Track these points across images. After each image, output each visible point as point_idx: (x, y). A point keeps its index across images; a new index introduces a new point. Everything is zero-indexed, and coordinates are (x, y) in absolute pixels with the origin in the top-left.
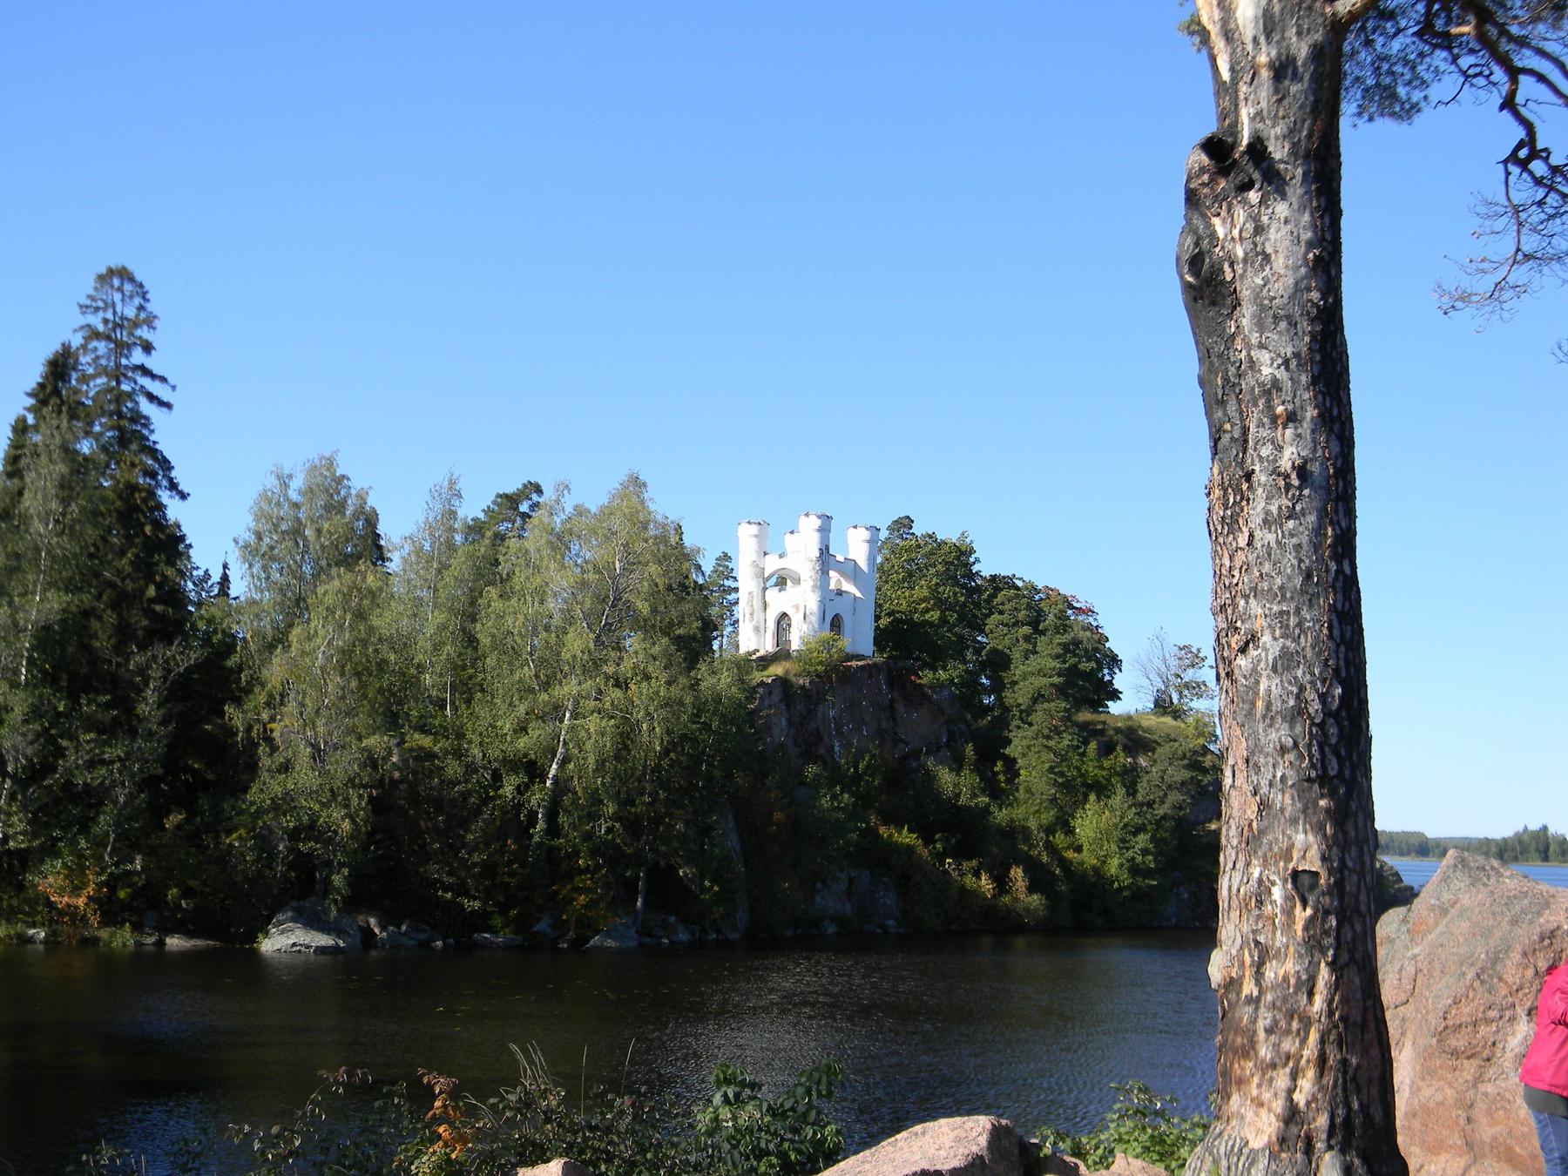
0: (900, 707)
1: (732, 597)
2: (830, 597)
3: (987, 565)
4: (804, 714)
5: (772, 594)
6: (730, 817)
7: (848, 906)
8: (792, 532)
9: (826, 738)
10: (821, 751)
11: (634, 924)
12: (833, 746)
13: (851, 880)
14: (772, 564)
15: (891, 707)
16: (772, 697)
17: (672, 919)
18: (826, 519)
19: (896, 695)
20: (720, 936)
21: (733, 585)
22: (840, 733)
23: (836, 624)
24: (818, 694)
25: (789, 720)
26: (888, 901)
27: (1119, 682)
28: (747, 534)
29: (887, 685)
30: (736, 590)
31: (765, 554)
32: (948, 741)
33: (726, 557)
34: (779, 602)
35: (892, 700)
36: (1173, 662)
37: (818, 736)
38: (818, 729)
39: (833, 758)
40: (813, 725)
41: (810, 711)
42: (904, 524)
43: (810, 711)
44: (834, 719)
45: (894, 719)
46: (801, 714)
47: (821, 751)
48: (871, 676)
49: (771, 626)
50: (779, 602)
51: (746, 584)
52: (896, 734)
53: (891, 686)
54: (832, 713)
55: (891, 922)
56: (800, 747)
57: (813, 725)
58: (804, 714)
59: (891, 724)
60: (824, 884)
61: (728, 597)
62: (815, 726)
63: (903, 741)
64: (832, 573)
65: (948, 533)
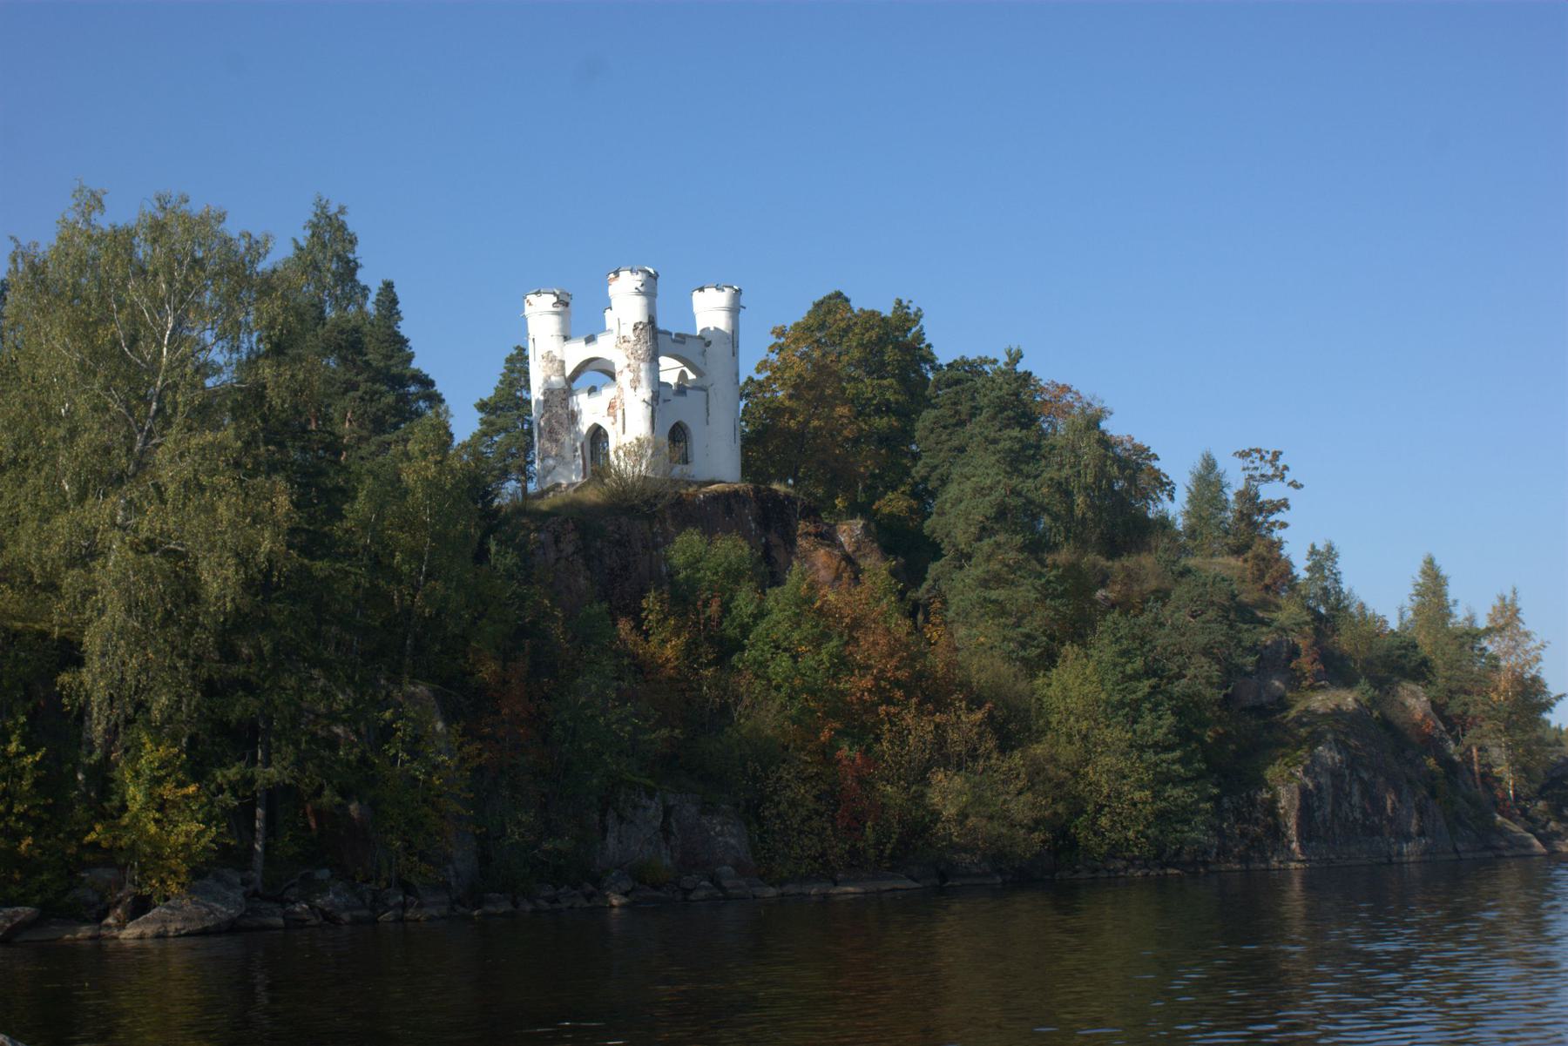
2: (660, 396)
13: (668, 811)
18: (652, 278)
19: (774, 538)
26: (733, 841)
28: (541, 316)
31: (566, 338)
60: (621, 819)
64: (665, 362)
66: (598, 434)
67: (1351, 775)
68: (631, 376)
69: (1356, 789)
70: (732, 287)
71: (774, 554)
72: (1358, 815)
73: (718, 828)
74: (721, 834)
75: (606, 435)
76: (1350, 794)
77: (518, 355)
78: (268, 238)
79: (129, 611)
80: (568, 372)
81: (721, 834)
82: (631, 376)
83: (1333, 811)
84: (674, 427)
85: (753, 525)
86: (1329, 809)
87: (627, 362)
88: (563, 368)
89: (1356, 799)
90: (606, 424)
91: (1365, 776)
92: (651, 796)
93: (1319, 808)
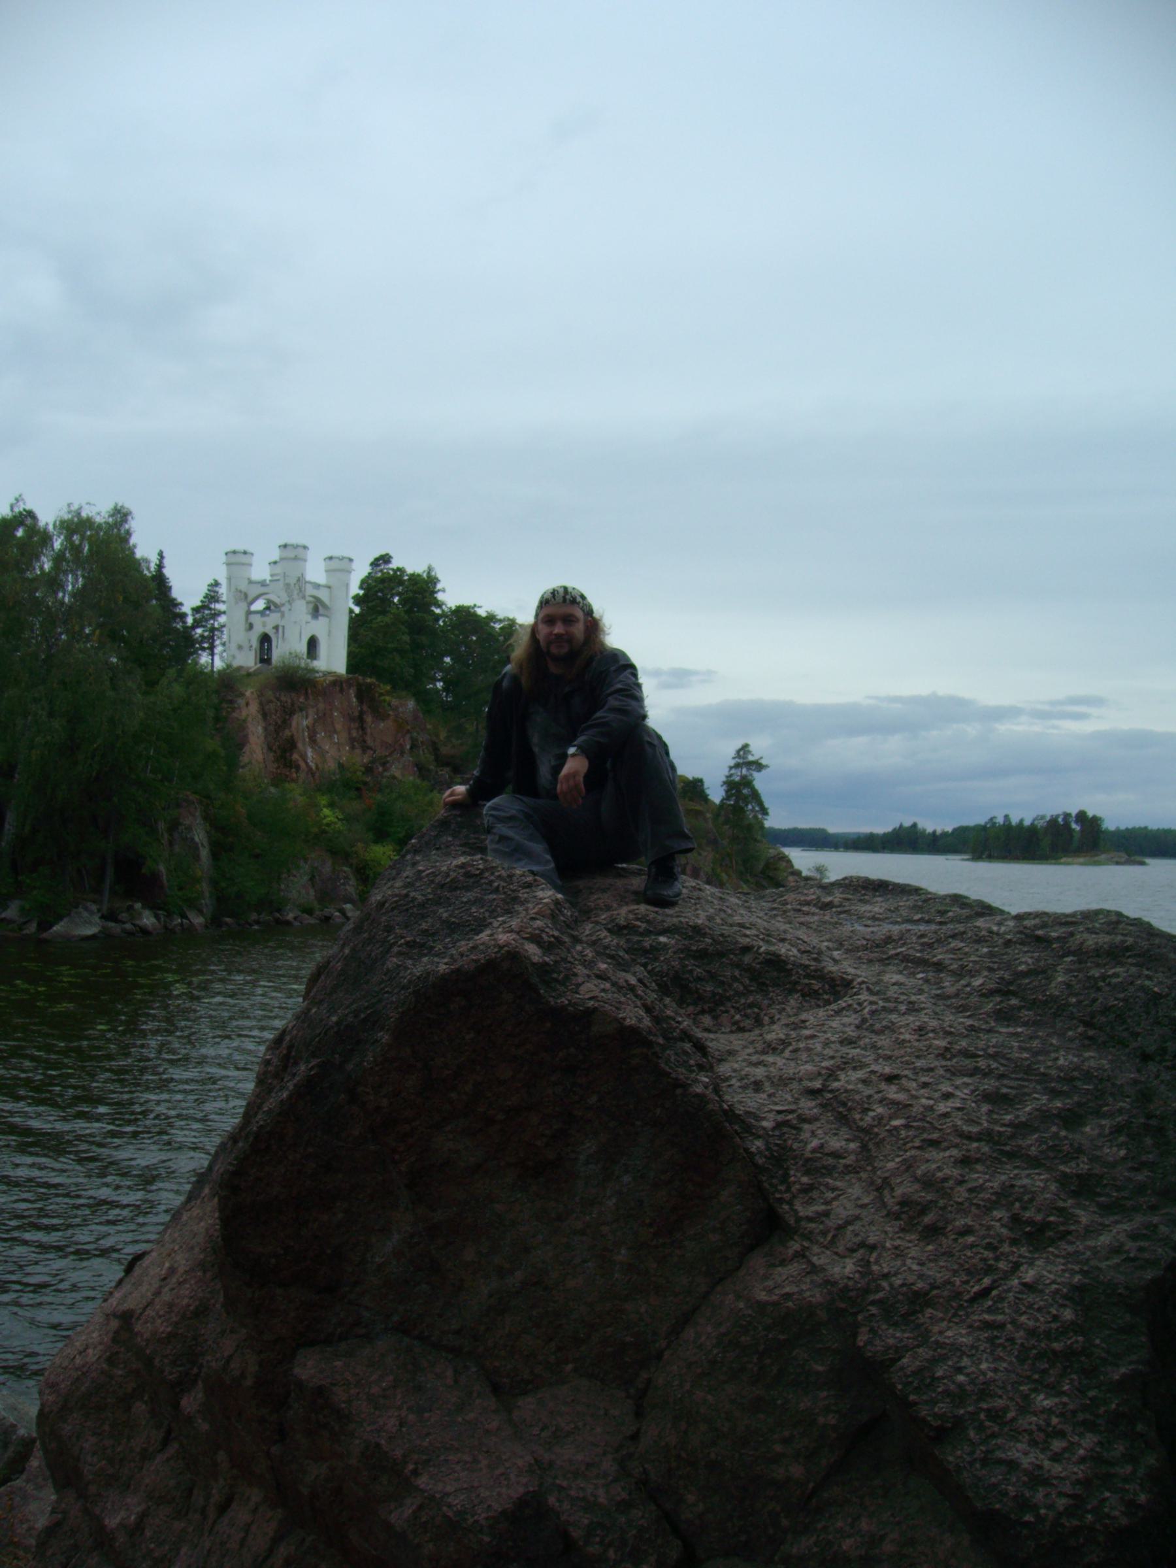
0: (369, 719)
1: (222, 619)
4: (279, 723)
6: (198, 814)
7: (312, 892)
8: (275, 563)
9: (300, 745)
10: (295, 756)
11: (99, 910)
12: (306, 753)
15: (361, 719)
17: (138, 906)
19: (365, 708)
20: (185, 921)
22: (313, 740)
23: (313, 643)
24: (293, 705)
25: (265, 729)
32: (411, 748)
33: (217, 584)
35: (362, 713)
37: (291, 745)
38: (292, 736)
39: (307, 763)
40: (287, 733)
41: (284, 722)
42: (385, 559)
43: (284, 722)
44: (308, 727)
45: (363, 729)
46: (276, 723)
47: (295, 756)
49: (255, 643)
52: (364, 741)
53: (360, 697)
54: (305, 723)
55: (348, 906)
56: (275, 752)
57: (287, 733)
58: (279, 723)
59: (360, 732)
62: (289, 734)
63: (369, 748)
66: (265, 639)
71: (365, 717)
73: (342, 881)
74: (344, 884)
80: (250, 598)
81: (344, 884)
85: (354, 700)
90: (271, 633)
92: (306, 863)
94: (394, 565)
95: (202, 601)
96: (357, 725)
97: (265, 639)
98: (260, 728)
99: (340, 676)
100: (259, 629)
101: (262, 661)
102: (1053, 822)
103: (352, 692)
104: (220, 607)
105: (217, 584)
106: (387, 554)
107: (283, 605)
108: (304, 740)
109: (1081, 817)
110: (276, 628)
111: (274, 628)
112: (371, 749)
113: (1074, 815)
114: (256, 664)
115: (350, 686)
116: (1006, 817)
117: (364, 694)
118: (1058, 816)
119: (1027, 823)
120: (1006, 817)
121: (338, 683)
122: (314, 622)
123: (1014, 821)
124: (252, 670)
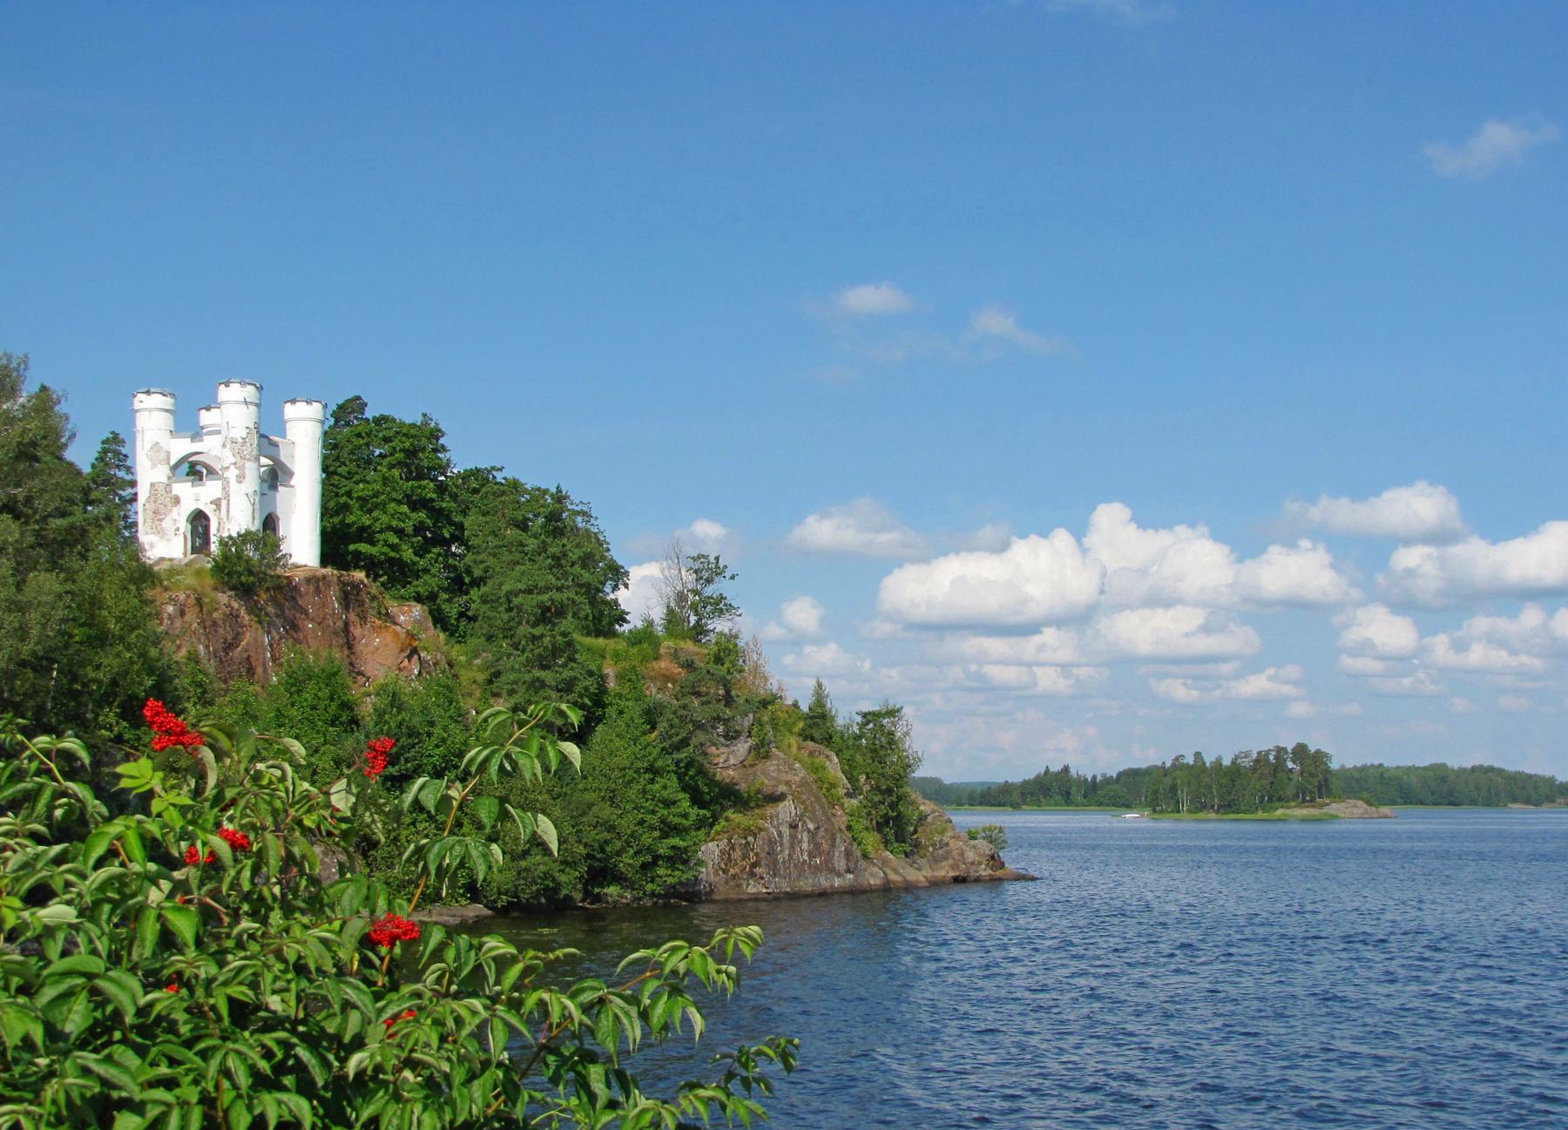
0: (356, 631)
3: (461, 456)
5: (184, 489)
14: (181, 447)
16: (187, 618)
19: (353, 617)
21: (128, 477)
27: (623, 597)
29: (340, 604)
30: (133, 484)
33: (116, 439)
34: (193, 496)
35: (346, 624)
36: (690, 578)
45: (350, 647)
48: (318, 591)
49: (184, 526)
50: (193, 496)
51: (148, 473)
59: (346, 652)
61: (121, 492)
63: (360, 673)
65: (408, 415)
66: (199, 520)
67: (803, 826)
68: (237, 472)
69: (805, 837)
70: (320, 402)
71: (352, 629)
72: (806, 858)
75: (207, 518)
76: (800, 841)
77: (114, 438)
78: (25, 360)
79: (887, 910)
80: (173, 462)
82: (237, 472)
83: (789, 855)
84: (266, 518)
86: (787, 852)
87: (234, 460)
88: (169, 458)
89: (805, 846)
90: (209, 510)
91: (811, 826)
93: (781, 851)
94: (370, 413)
95: (93, 466)
96: (341, 641)
97: (199, 520)
98: (201, 647)
99: (312, 569)
100: (187, 507)
101: (195, 550)
102: (1261, 759)
103: (333, 595)
104: (121, 474)
105: (116, 439)
106: (359, 398)
107: (228, 468)
108: (264, 664)
109: (1300, 751)
110: (217, 503)
111: (211, 503)
112: (364, 676)
113: (1289, 750)
114: (185, 554)
115: (328, 585)
116: (1198, 755)
117: (350, 595)
118: (1268, 752)
119: (1227, 762)
120: (1198, 755)
121: (313, 580)
122: (270, 493)
123: (1209, 760)
124: (183, 563)
